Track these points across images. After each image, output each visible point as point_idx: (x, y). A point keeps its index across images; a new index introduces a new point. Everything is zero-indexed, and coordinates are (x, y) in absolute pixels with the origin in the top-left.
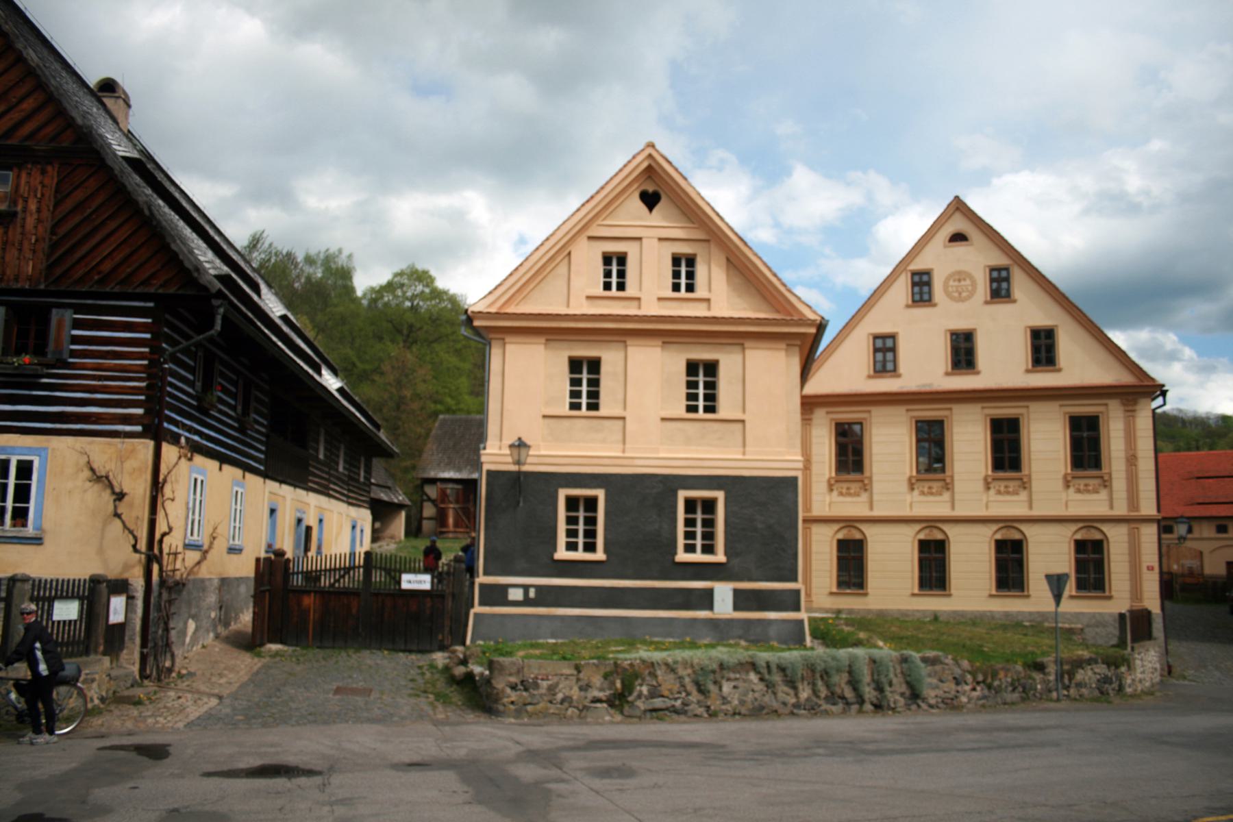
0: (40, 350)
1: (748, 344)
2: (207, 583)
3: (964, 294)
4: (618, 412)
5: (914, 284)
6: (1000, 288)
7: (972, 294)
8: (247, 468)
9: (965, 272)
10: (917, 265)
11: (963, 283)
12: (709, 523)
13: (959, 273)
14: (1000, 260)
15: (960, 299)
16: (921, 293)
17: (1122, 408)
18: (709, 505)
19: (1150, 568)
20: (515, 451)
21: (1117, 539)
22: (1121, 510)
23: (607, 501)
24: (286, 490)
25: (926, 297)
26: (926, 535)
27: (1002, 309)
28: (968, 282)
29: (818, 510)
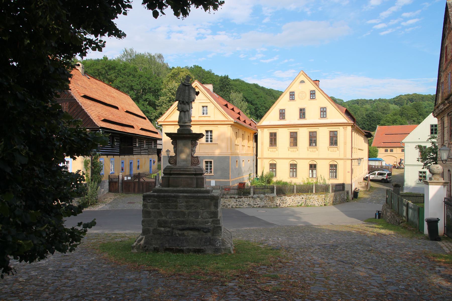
2: (105, 181)
3: (303, 98)
5: (290, 95)
8: (114, 155)
10: (291, 90)
11: (303, 95)
16: (292, 97)
20: (167, 152)
22: (342, 157)
24: (127, 157)
29: (265, 156)
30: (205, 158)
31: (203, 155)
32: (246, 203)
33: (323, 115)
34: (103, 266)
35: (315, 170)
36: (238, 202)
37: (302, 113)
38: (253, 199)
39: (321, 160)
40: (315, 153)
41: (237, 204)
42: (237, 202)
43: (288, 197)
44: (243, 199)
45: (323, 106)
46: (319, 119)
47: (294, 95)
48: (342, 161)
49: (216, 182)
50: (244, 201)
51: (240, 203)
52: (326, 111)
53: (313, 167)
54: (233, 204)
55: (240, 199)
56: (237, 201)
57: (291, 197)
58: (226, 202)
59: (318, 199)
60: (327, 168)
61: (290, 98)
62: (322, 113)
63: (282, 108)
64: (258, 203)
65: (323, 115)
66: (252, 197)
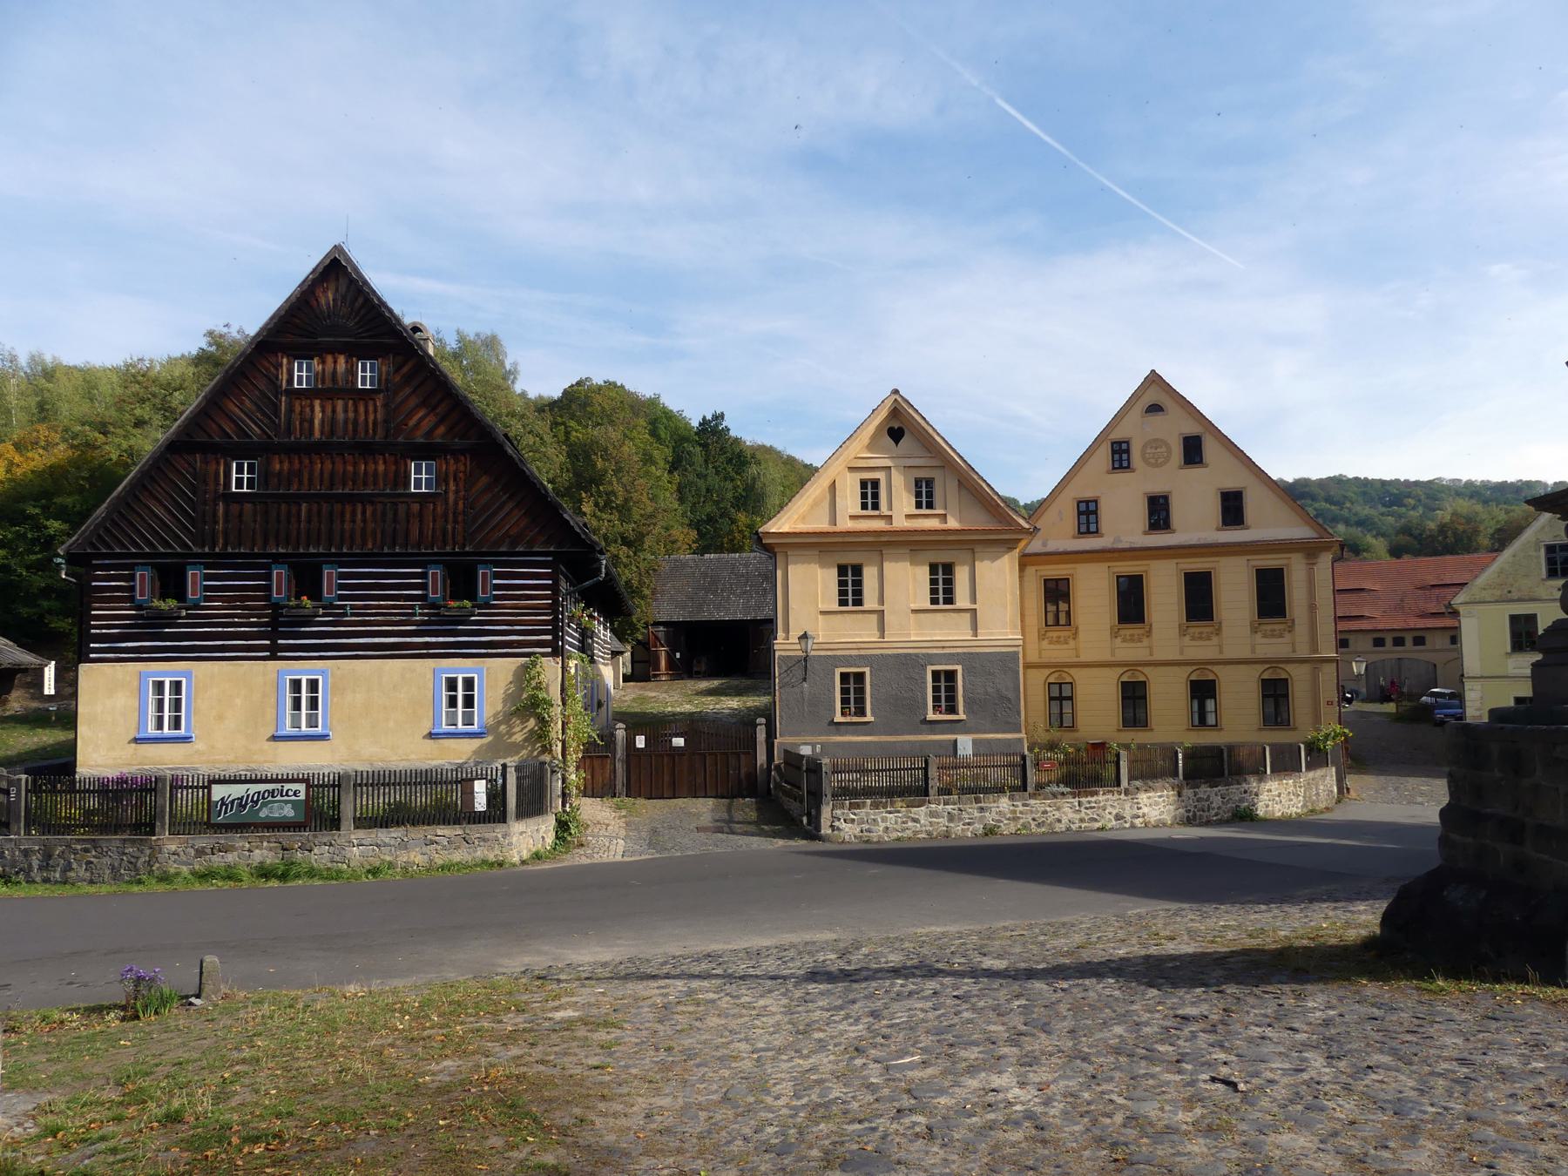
0: (472, 596)
1: (978, 549)
4: (876, 606)
5: (1114, 452)
6: (1193, 451)
7: (1167, 459)
9: (1162, 440)
10: (1117, 435)
11: (1159, 450)
12: (951, 689)
13: (1156, 440)
14: (1192, 429)
15: (1156, 465)
17: (1304, 561)
18: (951, 676)
19: (1330, 703)
21: (1299, 678)
22: (1303, 652)
23: (871, 675)
25: (1125, 464)
26: (1129, 677)
27: (1195, 472)
28: (1164, 449)
30: (931, 659)
31: (924, 651)
32: (1110, 813)
33: (1088, 523)
34: (1081, 1084)
35: (1213, 701)
36: (1086, 808)
37: (1159, 511)
38: (1130, 797)
39: (1228, 667)
40: (1065, 646)
41: (1083, 815)
42: (1082, 809)
43: (1211, 787)
44: (1101, 798)
45: (1231, 484)
46: (1218, 530)
47: (1128, 451)
48: (1306, 668)
49: (975, 742)
50: (1102, 804)
51: (1088, 811)
52: (1095, 512)
53: (1203, 691)
54: (1071, 815)
55: (1089, 799)
56: (1080, 804)
57: (1220, 788)
58: (1048, 809)
59: (1279, 795)
60: (1181, 692)
61: (1113, 461)
62: (1083, 518)
63: (1088, 494)
64: (1145, 810)
65: (1088, 523)
66: (1127, 792)
